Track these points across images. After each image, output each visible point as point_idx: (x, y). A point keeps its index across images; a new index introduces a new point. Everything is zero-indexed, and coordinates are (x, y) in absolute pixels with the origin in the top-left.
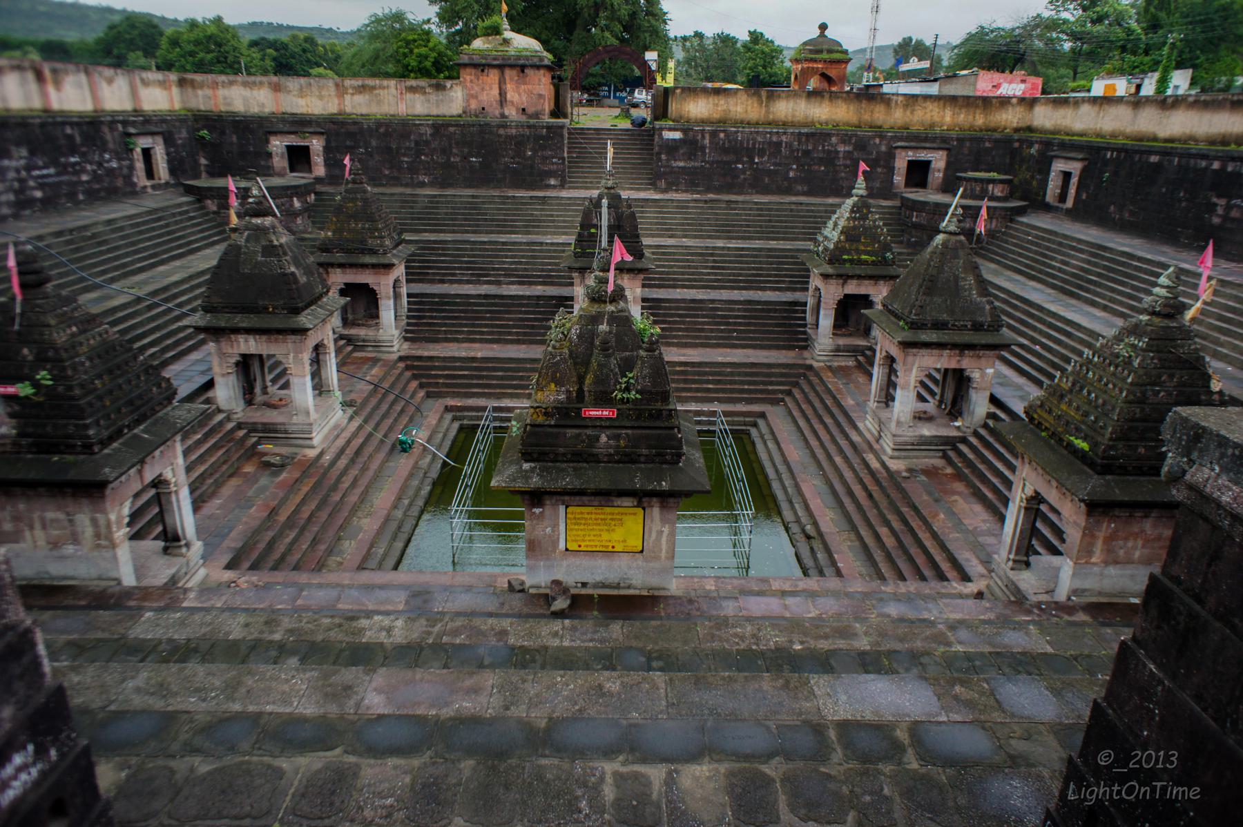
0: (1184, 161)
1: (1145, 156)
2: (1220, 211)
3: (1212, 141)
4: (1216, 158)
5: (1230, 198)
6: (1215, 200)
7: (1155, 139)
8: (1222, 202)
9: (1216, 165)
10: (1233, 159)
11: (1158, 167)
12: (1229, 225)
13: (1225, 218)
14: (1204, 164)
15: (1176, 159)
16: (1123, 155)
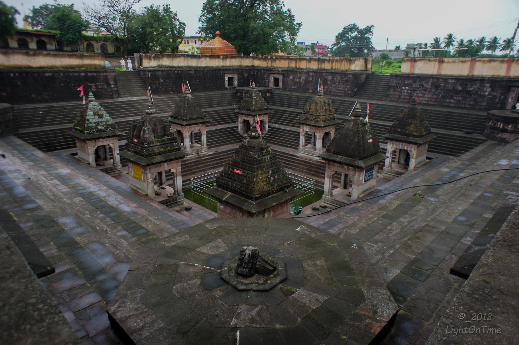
0: (66, 74)
1: (41, 74)
2: (94, 87)
3: (66, 67)
4: (83, 72)
5: (95, 83)
6: (90, 84)
7: (30, 67)
8: (93, 84)
9: (83, 74)
10: (90, 72)
11: (52, 77)
12: (99, 90)
13: (97, 88)
14: (77, 74)
15: (62, 74)
16: (24, 75)
